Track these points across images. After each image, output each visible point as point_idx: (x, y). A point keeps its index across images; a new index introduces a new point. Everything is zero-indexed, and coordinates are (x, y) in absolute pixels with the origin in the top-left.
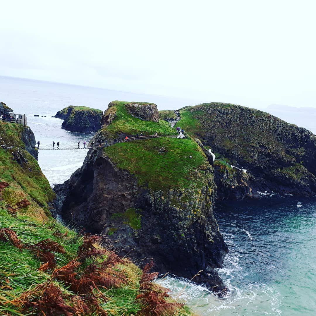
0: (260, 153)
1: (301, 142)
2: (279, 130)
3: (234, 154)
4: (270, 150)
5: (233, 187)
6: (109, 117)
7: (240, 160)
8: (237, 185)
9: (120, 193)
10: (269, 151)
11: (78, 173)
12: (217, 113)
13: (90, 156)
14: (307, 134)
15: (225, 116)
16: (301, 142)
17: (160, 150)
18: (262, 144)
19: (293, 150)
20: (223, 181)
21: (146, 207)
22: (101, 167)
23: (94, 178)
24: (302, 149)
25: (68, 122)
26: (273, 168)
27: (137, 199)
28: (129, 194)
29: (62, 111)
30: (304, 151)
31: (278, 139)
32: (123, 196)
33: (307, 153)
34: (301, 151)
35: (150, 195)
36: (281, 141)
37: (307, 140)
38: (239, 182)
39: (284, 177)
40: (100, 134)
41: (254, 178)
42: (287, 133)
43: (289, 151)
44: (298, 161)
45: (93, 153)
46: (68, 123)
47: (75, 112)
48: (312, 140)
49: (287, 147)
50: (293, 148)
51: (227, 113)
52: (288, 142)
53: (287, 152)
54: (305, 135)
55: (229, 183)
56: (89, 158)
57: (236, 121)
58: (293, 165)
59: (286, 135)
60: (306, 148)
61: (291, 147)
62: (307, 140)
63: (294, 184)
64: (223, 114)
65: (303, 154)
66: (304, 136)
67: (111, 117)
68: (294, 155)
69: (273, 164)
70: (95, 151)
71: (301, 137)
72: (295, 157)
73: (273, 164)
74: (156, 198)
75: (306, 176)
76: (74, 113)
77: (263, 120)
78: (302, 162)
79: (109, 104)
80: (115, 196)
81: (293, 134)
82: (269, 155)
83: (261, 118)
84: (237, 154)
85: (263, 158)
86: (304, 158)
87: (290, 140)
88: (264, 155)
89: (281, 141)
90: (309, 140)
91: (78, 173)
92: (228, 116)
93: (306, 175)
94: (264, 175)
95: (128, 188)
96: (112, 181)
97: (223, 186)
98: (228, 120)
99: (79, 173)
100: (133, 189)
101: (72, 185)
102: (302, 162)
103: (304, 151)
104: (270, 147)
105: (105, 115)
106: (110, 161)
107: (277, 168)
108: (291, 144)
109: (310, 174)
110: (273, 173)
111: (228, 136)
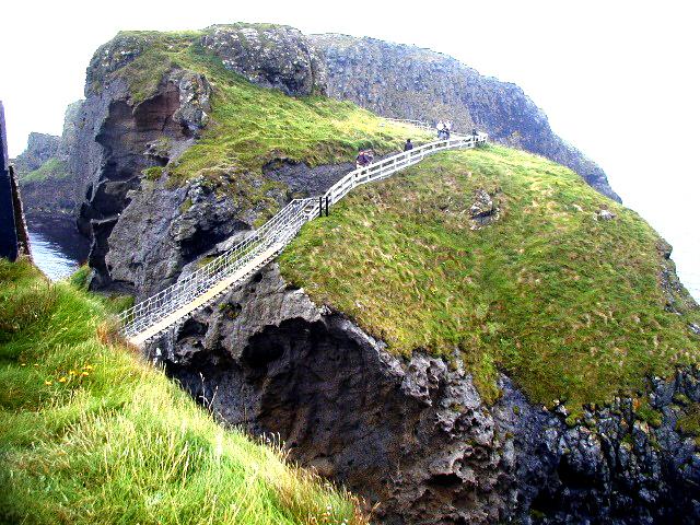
9: (419, 472)
12: (329, 64)
15: (349, 71)
17: (475, 211)
21: (567, 492)
27: (507, 469)
28: (465, 462)
32: (445, 482)
35: (574, 434)
40: (204, 188)
51: (354, 62)
54: (518, 99)
57: (379, 82)
64: (343, 63)
67: (194, 98)
74: (610, 442)
77: (439, 71)
80: (398, 492)
81: (498, 101)
83: (434, 67)
95: (447, 434)
98: (361, 80)
100: (470, 428)
105: (128, 98)
106: (354, 329)
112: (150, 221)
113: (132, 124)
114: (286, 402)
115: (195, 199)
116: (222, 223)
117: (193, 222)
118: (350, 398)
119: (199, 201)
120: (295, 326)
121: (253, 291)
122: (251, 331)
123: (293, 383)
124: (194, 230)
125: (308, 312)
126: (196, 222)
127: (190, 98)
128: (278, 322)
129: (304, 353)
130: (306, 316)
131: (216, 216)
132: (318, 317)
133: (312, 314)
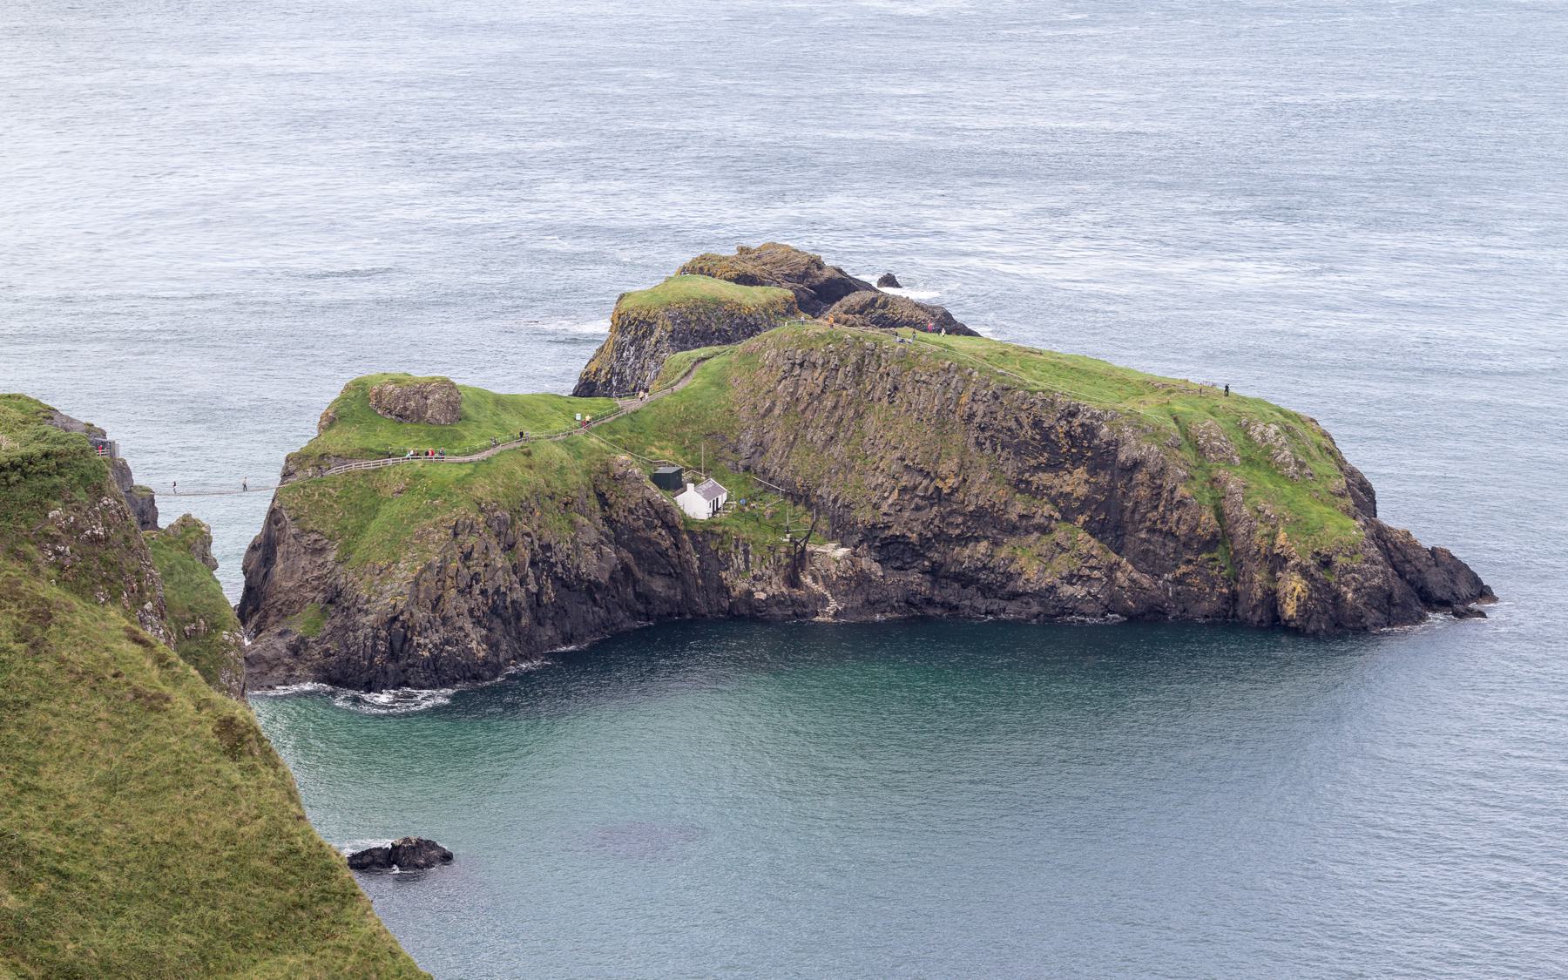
0: (904, 490)
1: (1073, 450)
2: (980, 413)
3: (825, 496)
4: (943, 480)
5: (763, 596)
7: (839, 516)
8: (777, 587)
10: (940, 484)
14: (1088, 422)
16: (1073, 450)
18: (912, 460)
19: (1044, 478)
20: (726, 579)
24: (1080, 473)
26: (963, 540)
30: (1087, 482)
31: (979, 444)
33: (1097, 488)
34: (1075, 482)
36: (995, 451)
37: (1090, 443)
38: (793, 582)
39: (1001, 570)
41: (880, 573)
42: (1013, 424)
43: (1028, 483)
44: (1067, 517)
48: (1108, 444)
49: (1018, 468)
50: (1044, 471)
52: (1020, 449)
53: (1021, 485)
54: (1082, 425)
55: (742, 585)
58: (1044, 530)
59: (1009, 429)
60: (1092, 471)
61: (1037, 468)
62: (1090, 443)
63: (1025, 594)
65: (1082, 490)
66: (1080, 430)
68: (1048, 495)
69: (958, 526)
71: (1068, 434)
72: (1054, 501)
73: (958, 526)
75: (1092, 568)
78: (1082, 519)
81: (1037, 424)
82: (937, 497)
84: (831, 498)
85: (918, 508)
86: (1086, 503)
87: (1026, 443)
88: (923, 498)
89: (995, 451)
90: (1096, 442)
92: (816, 375)
93: (1093, 562)
94: (926, 563)
97: (728, 592)
102: (1082, 519)
103: (1087, 482)
104: (943, 469)
107: (978, 540)
108: (1036, 458)
109: (1114, 557)
110: (962, 560)
111: (815, 439)
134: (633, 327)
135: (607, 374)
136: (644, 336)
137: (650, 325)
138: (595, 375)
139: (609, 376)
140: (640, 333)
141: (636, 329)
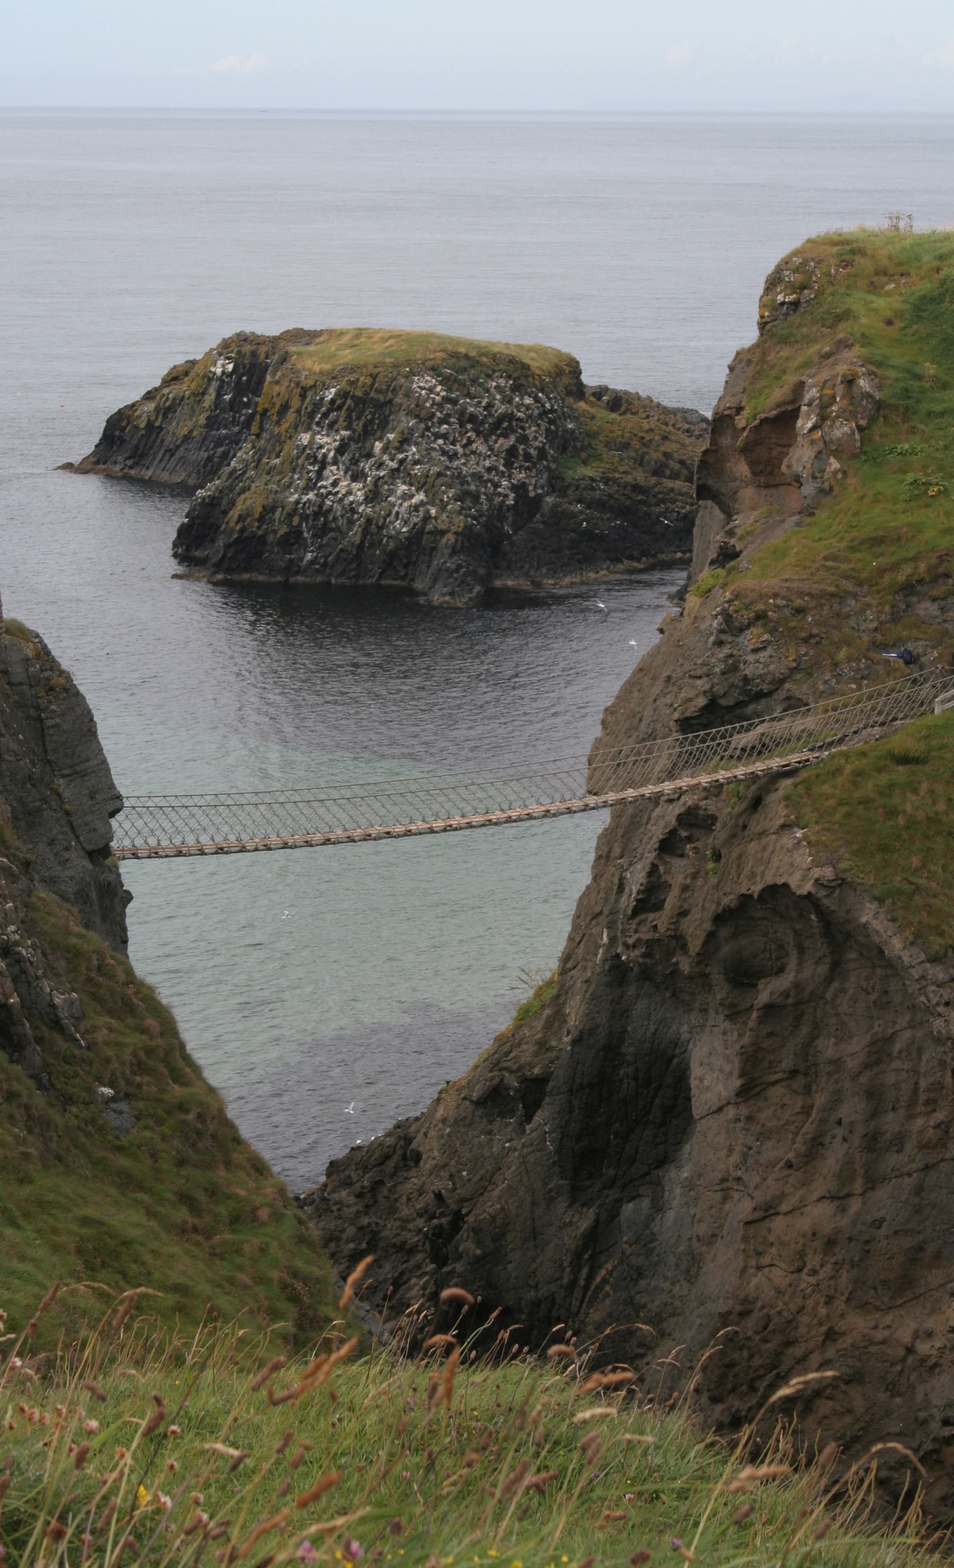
6: (805, 423)
11: (513, 1082)
13: (636, 878)
22: (766, 992)
23: (700, 1127)
25: (234, 514)
29: (151, 406)
45: (668, 846)
46: (241, 518)
47: (295, 403)
56: (627, 902)
70: (680, 818)
76: (285, 408)
79: (773, 282)
91: (513, 1082)
96: (909, 1147)
99: (524, 1080)
101: (458, 1219)
105: (739, 409)
112: (669, 678)
113: (742, 468)
114: (793, 1073)
115: (712, 639)
116: (759, 696)
117: (703, 684)
118: (890, 1078)
119: (719, 643)
120: (776, 891)
121: (745, 827)
122: (719, 903)
123: (804, 1031)
124: (702, 701)
125: (797, 876)
126: (707, 687)
127: (809, 425)
128: (757, 889)
129: (823, 969)
130: (793, 882)
131: (746, 679)
132: (808, 887)
133: (804, 879)
134: (343, 413)
135: (290, 516)
136: (368, 434)
137: (380, 406)
138: (261, 519)
139: (296, 520)
140: (359, 426)
141: (349, 417)
